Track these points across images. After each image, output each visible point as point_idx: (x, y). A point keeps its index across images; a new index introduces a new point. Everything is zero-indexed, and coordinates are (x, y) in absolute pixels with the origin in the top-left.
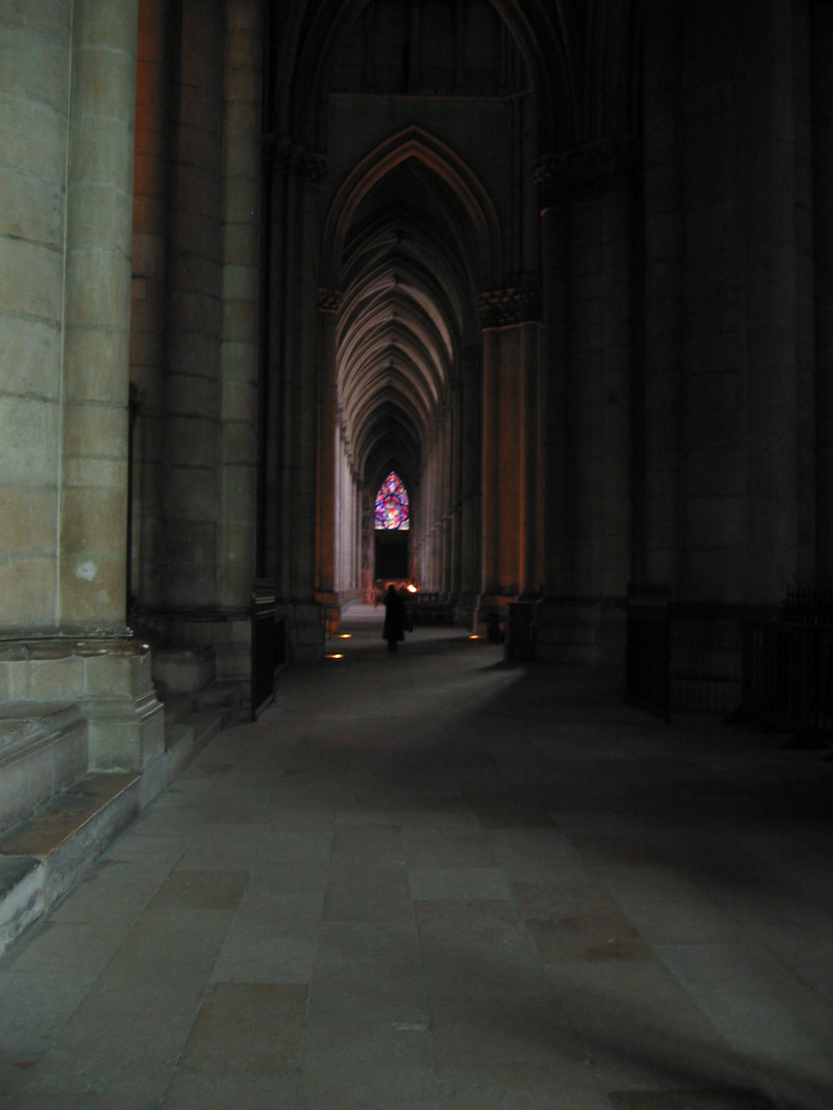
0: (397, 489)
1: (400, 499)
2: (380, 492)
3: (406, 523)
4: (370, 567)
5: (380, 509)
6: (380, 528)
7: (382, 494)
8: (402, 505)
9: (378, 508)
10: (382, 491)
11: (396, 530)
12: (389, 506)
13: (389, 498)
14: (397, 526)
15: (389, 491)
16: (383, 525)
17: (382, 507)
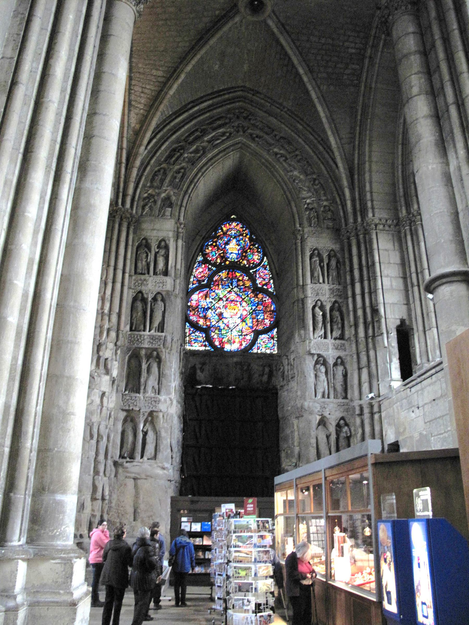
0: (243, 253)
1: (252, 279)
2: (200, 258)
3: (272, 338)
4: (165, 453)
5: (198, 301)
6: (197, 347)
7: (205, 261)
8: (257, 290)
9: (195, 297)
10: (205, 255)
11: (245, 352)
12: (221, 292)
13: (223, 274)
14: (244, 344)
15: (224, 257)
16: (209, 340)
17: (206, 296)
